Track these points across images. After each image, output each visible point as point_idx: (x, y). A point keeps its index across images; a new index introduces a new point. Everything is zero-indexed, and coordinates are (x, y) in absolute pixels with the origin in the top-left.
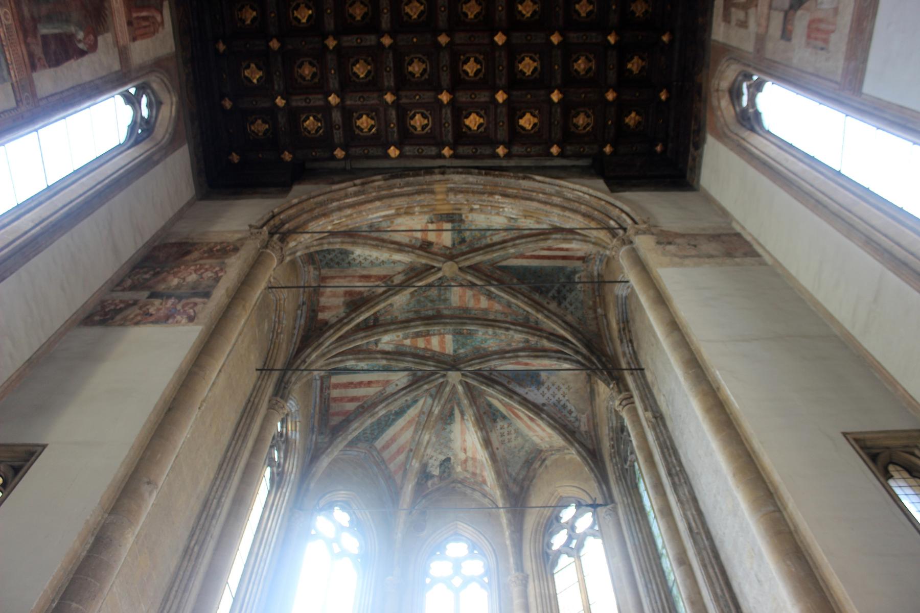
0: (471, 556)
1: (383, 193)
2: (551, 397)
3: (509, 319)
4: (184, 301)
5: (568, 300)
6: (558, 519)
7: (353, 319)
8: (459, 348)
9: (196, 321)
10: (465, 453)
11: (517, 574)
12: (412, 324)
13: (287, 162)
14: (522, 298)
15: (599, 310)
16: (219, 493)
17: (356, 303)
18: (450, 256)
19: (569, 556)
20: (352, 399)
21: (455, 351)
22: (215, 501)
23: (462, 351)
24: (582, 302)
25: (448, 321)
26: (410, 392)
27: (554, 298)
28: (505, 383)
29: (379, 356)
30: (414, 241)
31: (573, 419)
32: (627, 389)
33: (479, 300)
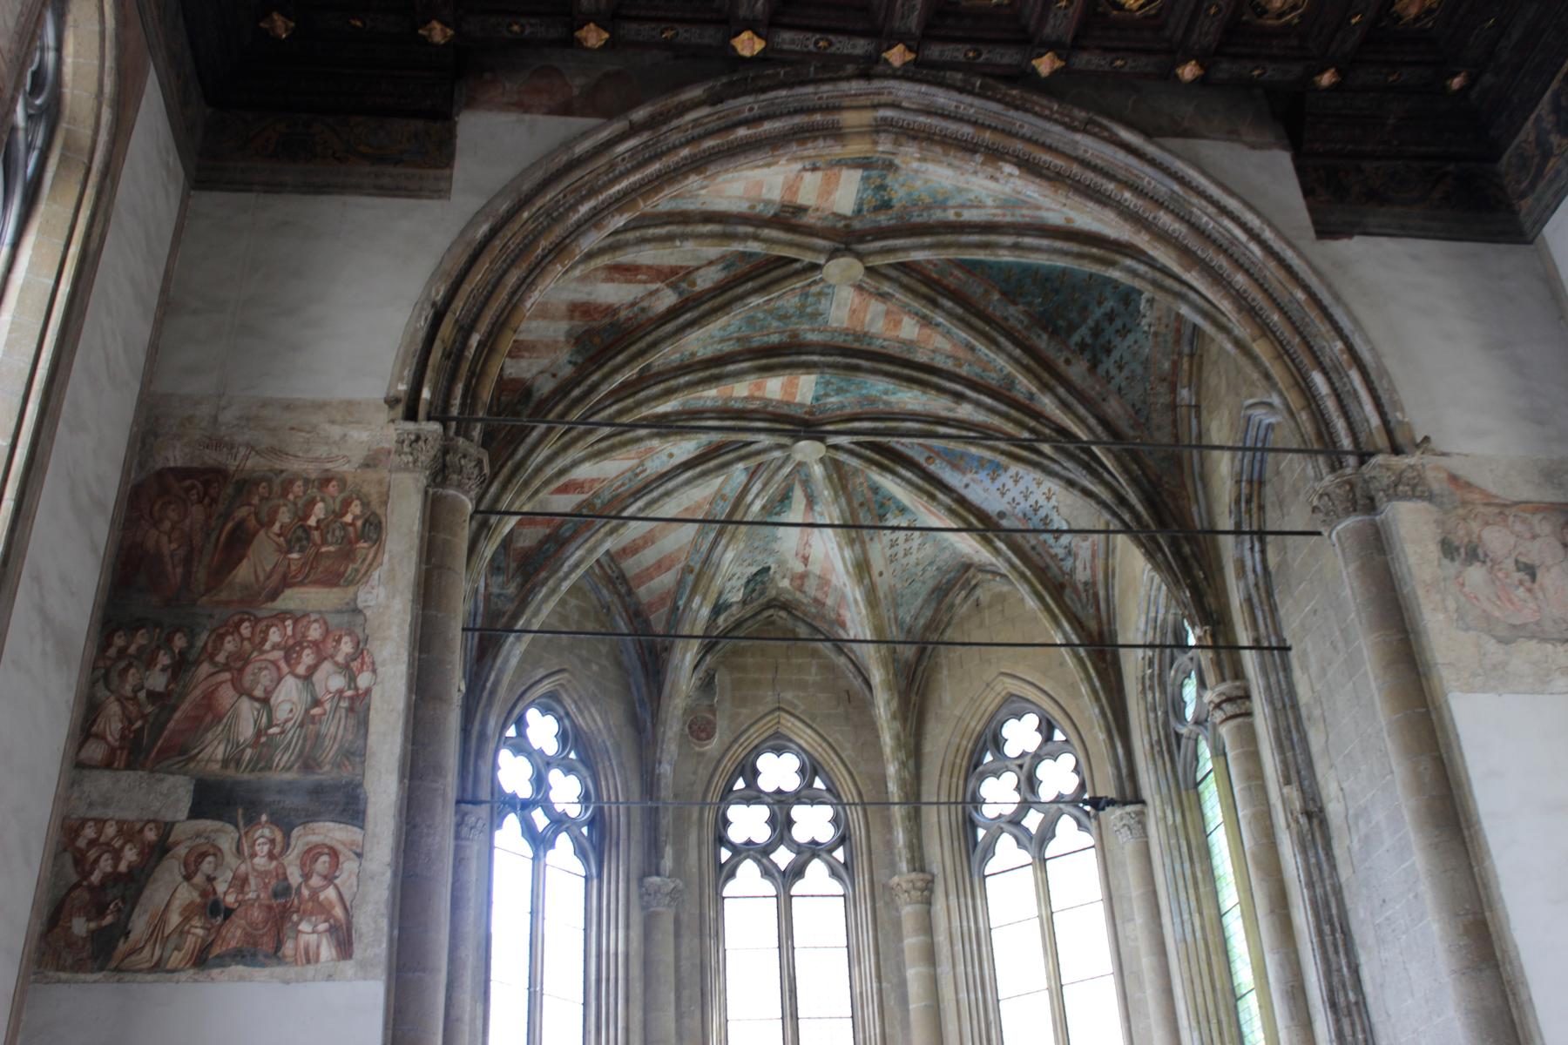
0: (805, 796)
1: (709, 143)
2: (1020, 498)
3: (964, 371)
4: (302, 838)
5: (1115, 355)
6: (997, 743)
7: (594, 388)
8: (827, 395)
11: (913, 875)
12: (731, 368)
13: (437, 45)
14: (1009, 346)
15: (1184, 394)
17: (604, 339)
18: (846, 238)
21: (817, 399)
23: (833, 399)
24: (1146, 364)
25: (815, 358)
26: (703, 474)
27: (1082, 347)
28: (921, 460)
29: (642, 432)
30: (760, 207)
31: (1061, 552)
32: (1239, 674)
33: (898, 323)
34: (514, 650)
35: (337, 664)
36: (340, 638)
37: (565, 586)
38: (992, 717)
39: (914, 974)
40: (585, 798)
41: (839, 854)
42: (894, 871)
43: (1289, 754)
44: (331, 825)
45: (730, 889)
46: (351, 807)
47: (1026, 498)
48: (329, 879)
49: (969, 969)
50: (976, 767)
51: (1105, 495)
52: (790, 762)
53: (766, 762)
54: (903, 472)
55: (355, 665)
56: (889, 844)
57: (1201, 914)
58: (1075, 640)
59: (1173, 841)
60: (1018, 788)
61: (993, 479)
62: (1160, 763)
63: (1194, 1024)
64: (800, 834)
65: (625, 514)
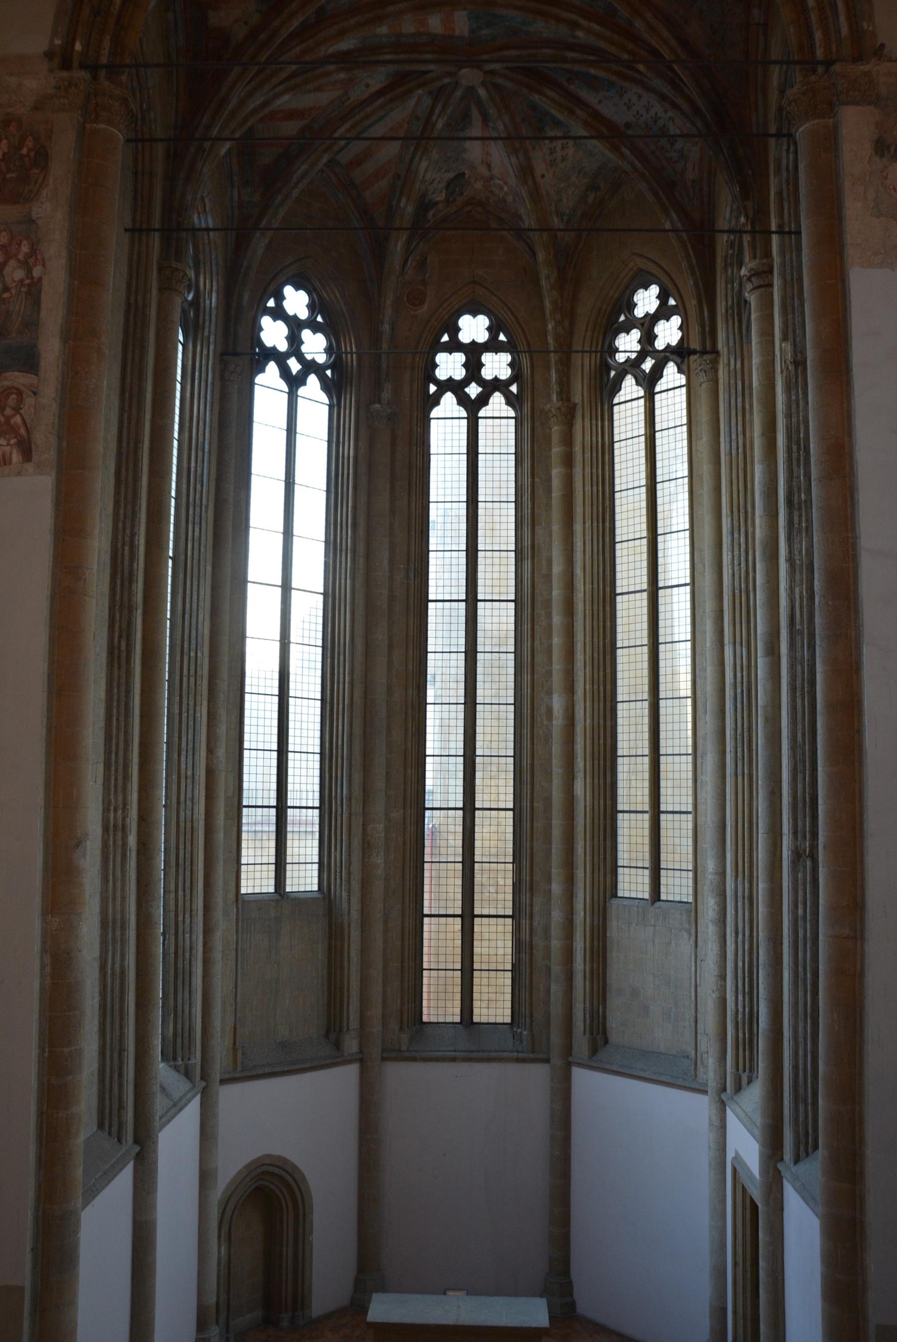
0: (492, 346)
9: (35, 457)
10: (490, 171)
16: (128, 531)
19: (638, 384)
20: (291, 115)
22: (127, 548)
32: (768, 254)
34: (259, 244)
35: (19, 260)
36: (21, 241)
37: (295, 193)
38: (626, 288)
39: (556, 473)
40: (328, 350)
41: (514, 388)
42: (549, 400)
43: (790, 317)
44: (17, 373)
45: (435, 413)
46: (29, 361)
47: (648, 111)
48: (17, 410)
49: (594, 470)
50: (612, 325)
51: (685, 106)
52: (483, 321)
53: (465, 321)
54: (549, 92)
55: (31, 261)
56: (547, 381)
57: (744, 435)
58: (679, 225)
59: (732, 382)
60: (639, 342)
61: (621, 96)
62: (730, 323)
63: (729, 513)
64: (487, 373)
65: (336, 135)
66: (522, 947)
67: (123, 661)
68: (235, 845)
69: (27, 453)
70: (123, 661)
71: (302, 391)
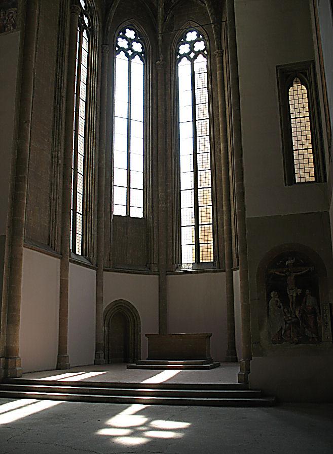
0: (198, 40)
34: (113, 12)
40: (142, 48)
41: (205, 52)
48: (12, 17)
52: (195, 33)
64: (196, 49)
66: (215, 233)
67: (58, 111)
68: (109, 194)
69: (14, 28)
70: (58, 111)
71: (133, 60)
